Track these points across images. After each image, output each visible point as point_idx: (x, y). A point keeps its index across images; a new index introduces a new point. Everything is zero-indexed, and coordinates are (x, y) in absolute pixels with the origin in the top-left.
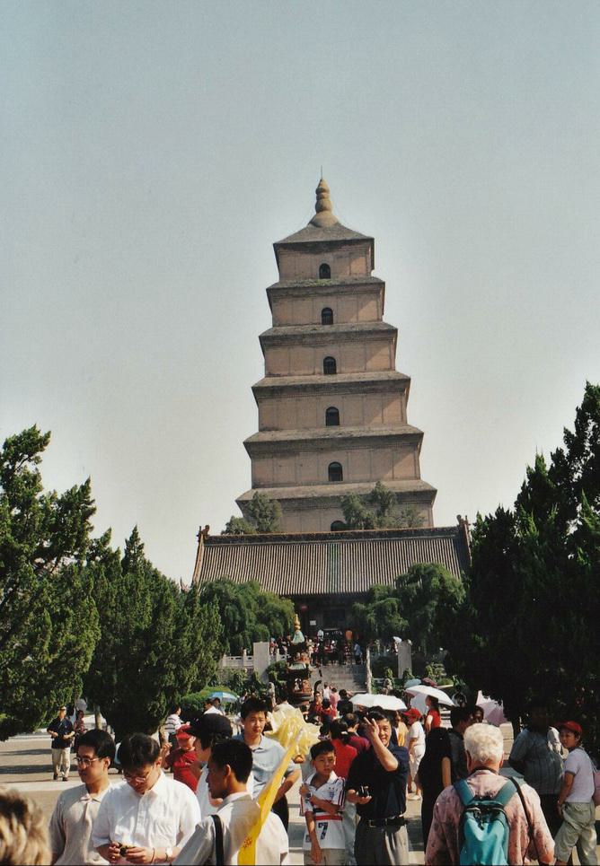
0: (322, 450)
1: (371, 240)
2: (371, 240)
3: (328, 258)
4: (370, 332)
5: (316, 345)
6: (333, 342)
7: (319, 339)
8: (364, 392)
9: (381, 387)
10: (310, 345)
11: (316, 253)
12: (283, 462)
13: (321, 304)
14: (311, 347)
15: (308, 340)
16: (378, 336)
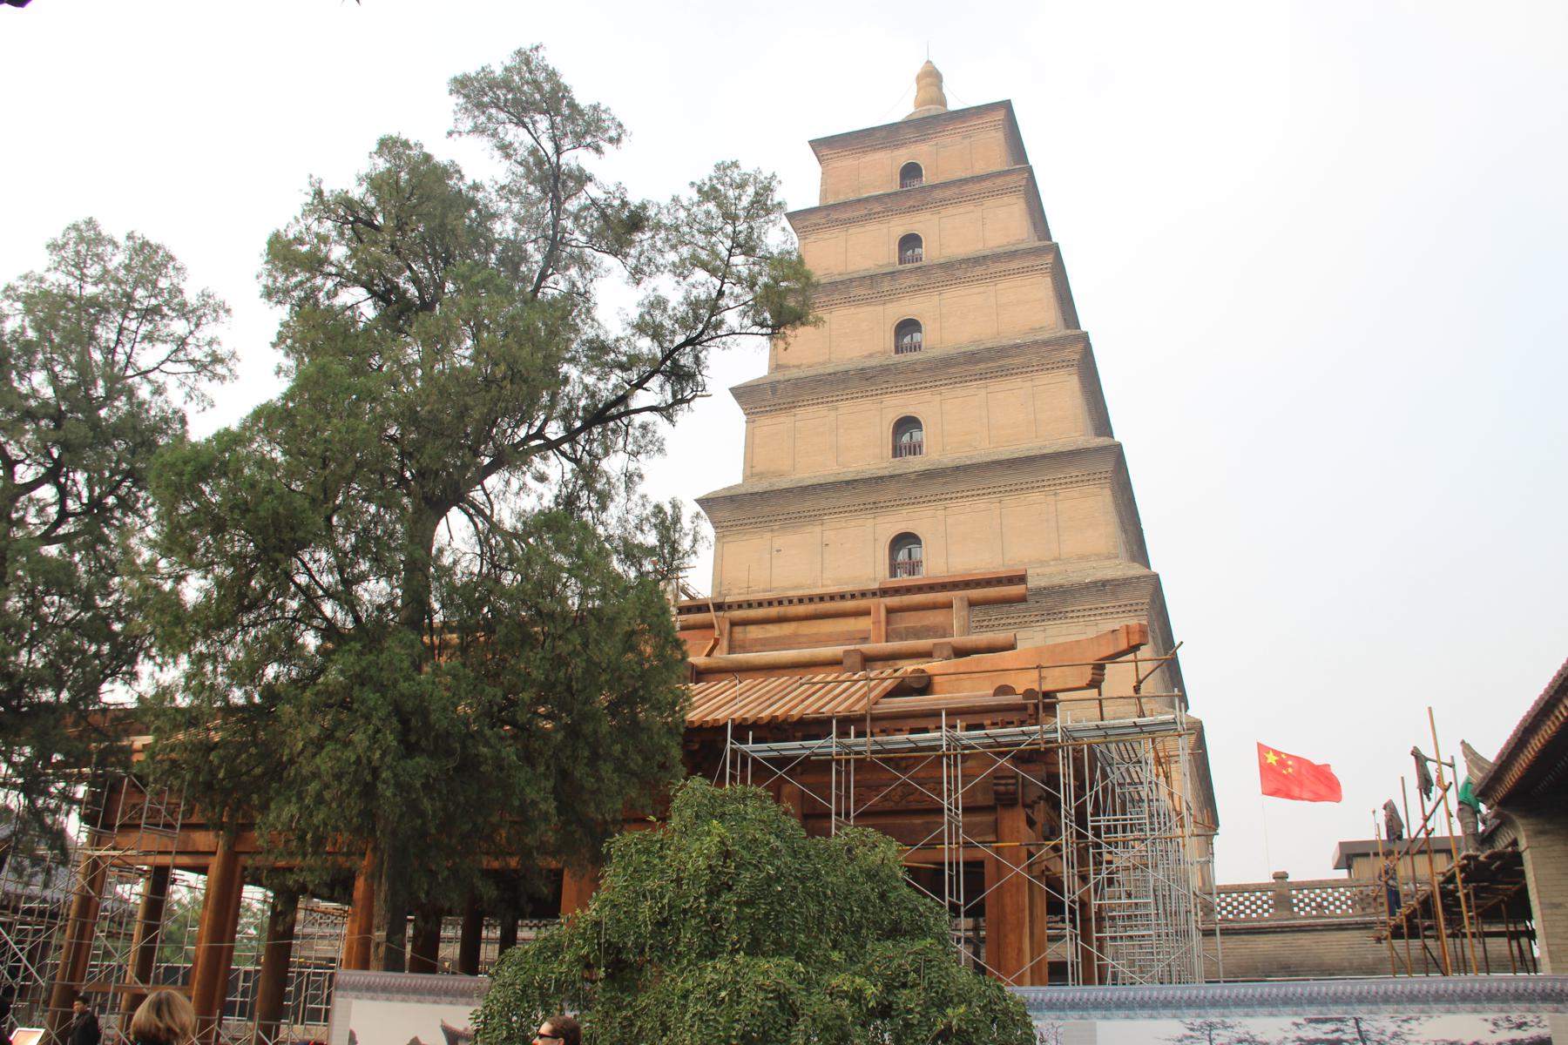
0: (876, 507)
1: (1006, 106)
2: (1006, 106)
3: (918, 152)
4: (996, 257)
5: (883, 298)
6: (917, 289)
7: (886, 286)
8: (982, 376)
9: (1018, 360)
10: (865, 301)
11: (897, 147)
12: (781, 540)
13: (900, 226)
14: (869, 304)
15: (861, 291)
16: (1014, 265)
